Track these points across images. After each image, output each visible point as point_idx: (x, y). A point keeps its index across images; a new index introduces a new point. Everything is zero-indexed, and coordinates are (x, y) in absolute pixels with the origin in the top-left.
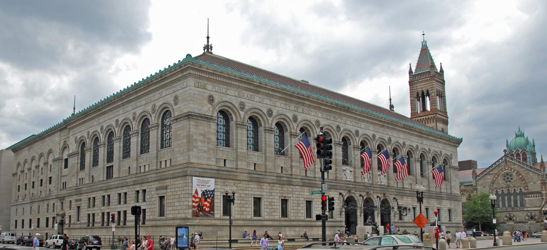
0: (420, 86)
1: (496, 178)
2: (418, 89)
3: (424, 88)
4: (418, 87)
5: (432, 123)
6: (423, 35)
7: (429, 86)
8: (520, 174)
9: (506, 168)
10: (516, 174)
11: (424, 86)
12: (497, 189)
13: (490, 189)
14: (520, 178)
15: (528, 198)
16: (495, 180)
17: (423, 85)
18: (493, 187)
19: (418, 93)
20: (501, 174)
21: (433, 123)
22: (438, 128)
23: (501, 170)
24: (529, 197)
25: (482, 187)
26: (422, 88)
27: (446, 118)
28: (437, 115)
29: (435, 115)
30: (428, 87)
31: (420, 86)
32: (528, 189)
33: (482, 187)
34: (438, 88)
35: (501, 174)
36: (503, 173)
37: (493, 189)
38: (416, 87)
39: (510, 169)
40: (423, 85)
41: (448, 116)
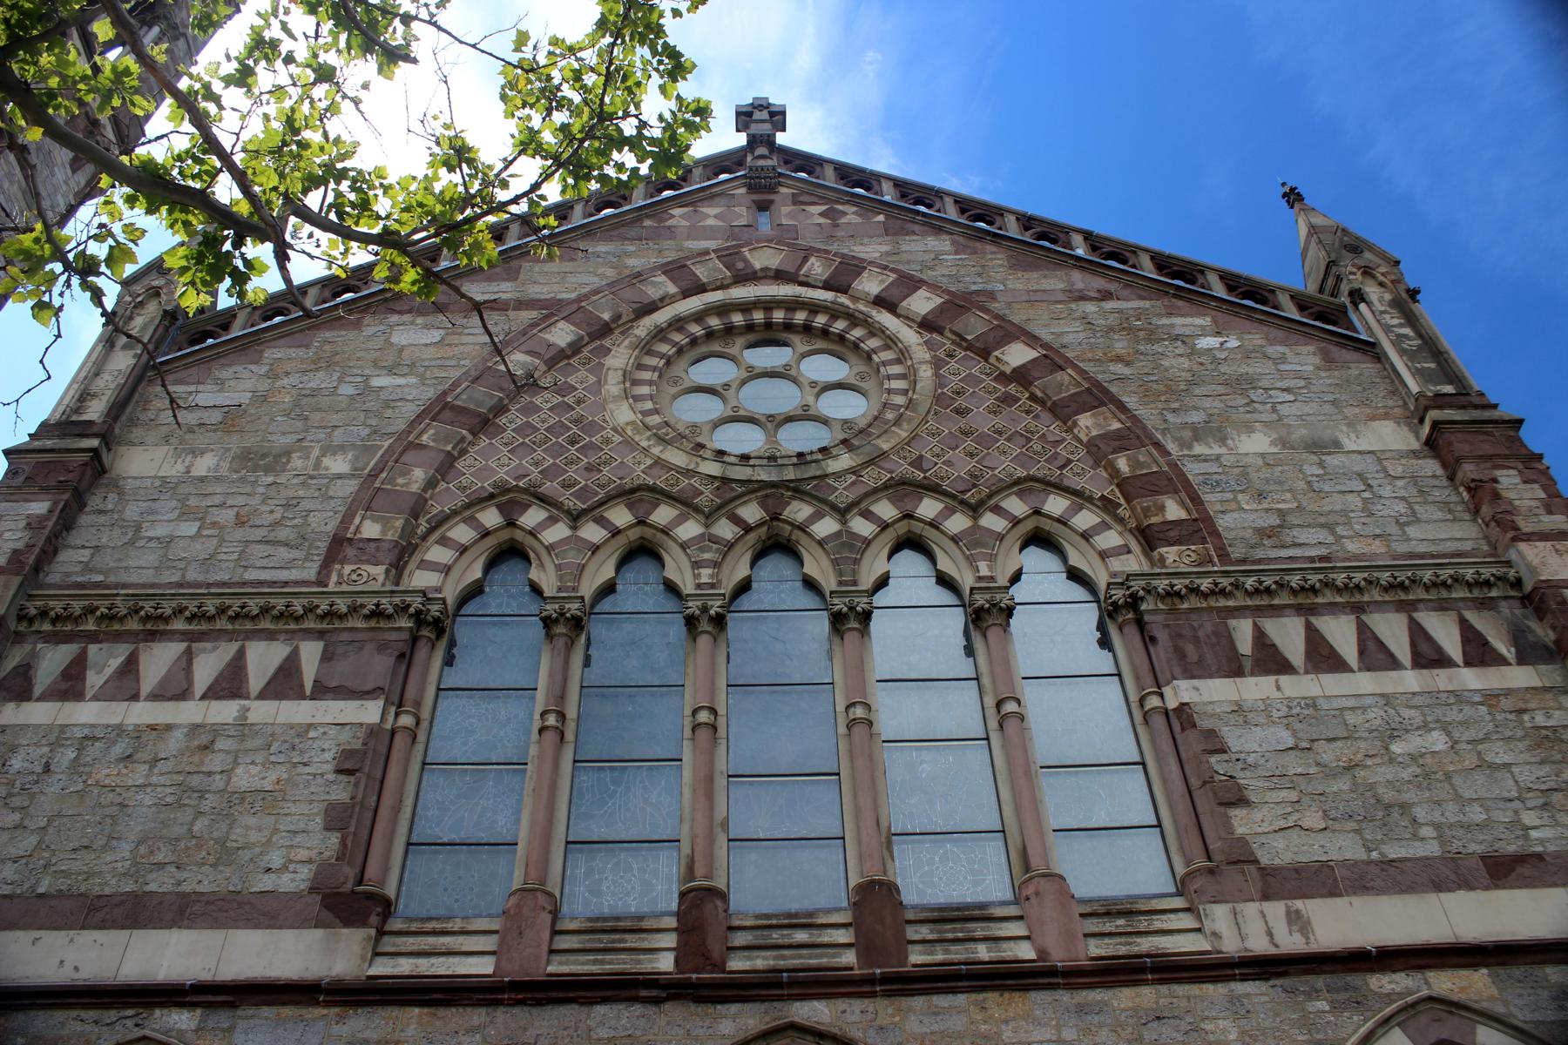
1: (560, 357)
8: (1009, 332)
9: (762, 259)
10: (927, 325)
12: (532, 517)
13: (369, 497)
14: (1003, 378)
15: (1234, 668)
16: (530, 384)
18: (446, 467)
20: (662, 317)
23: (674, 270)
24: (1270, 660)
32: (1199, 528)
35: (662, 317)
36: (694, 303)
37: (447, 498)
39: (817, 268)
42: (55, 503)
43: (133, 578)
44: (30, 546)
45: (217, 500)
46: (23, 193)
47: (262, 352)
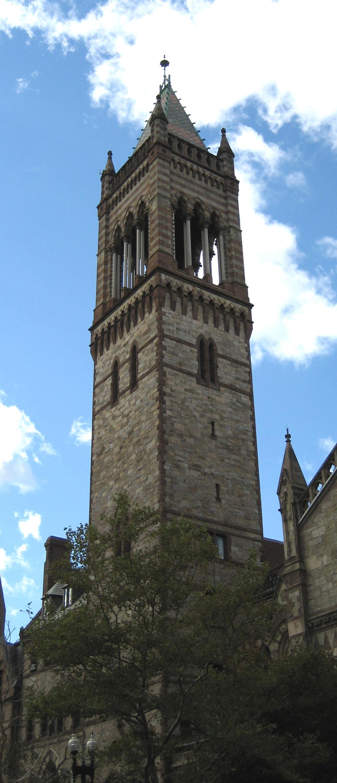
0: (128, 199)
2: (120, 215)
3: (134, 204)
4: (119, 212)
5: (147, 315)
6: (165, 63)
7: (148, 185)
11: (137, 193)
17: (131, 195)
19: (119, 227)
21: (150, 312)
22: (164, 327)
25: (325, 559)
26: (129, 207)
27: (246, 309)
28: (163, 276)
29: (153, 278)
30: (144, 193)
31: (128, 199)
33: (325, 559)
34: (186, 191)
38: (116, 212)
40: (131, 195)
41: (251, 302)
42: (300, 590)
43: (326, 607)
44: (301, 607)
45: (332, 572)
46: (232, 365)
47: (320, 507)
